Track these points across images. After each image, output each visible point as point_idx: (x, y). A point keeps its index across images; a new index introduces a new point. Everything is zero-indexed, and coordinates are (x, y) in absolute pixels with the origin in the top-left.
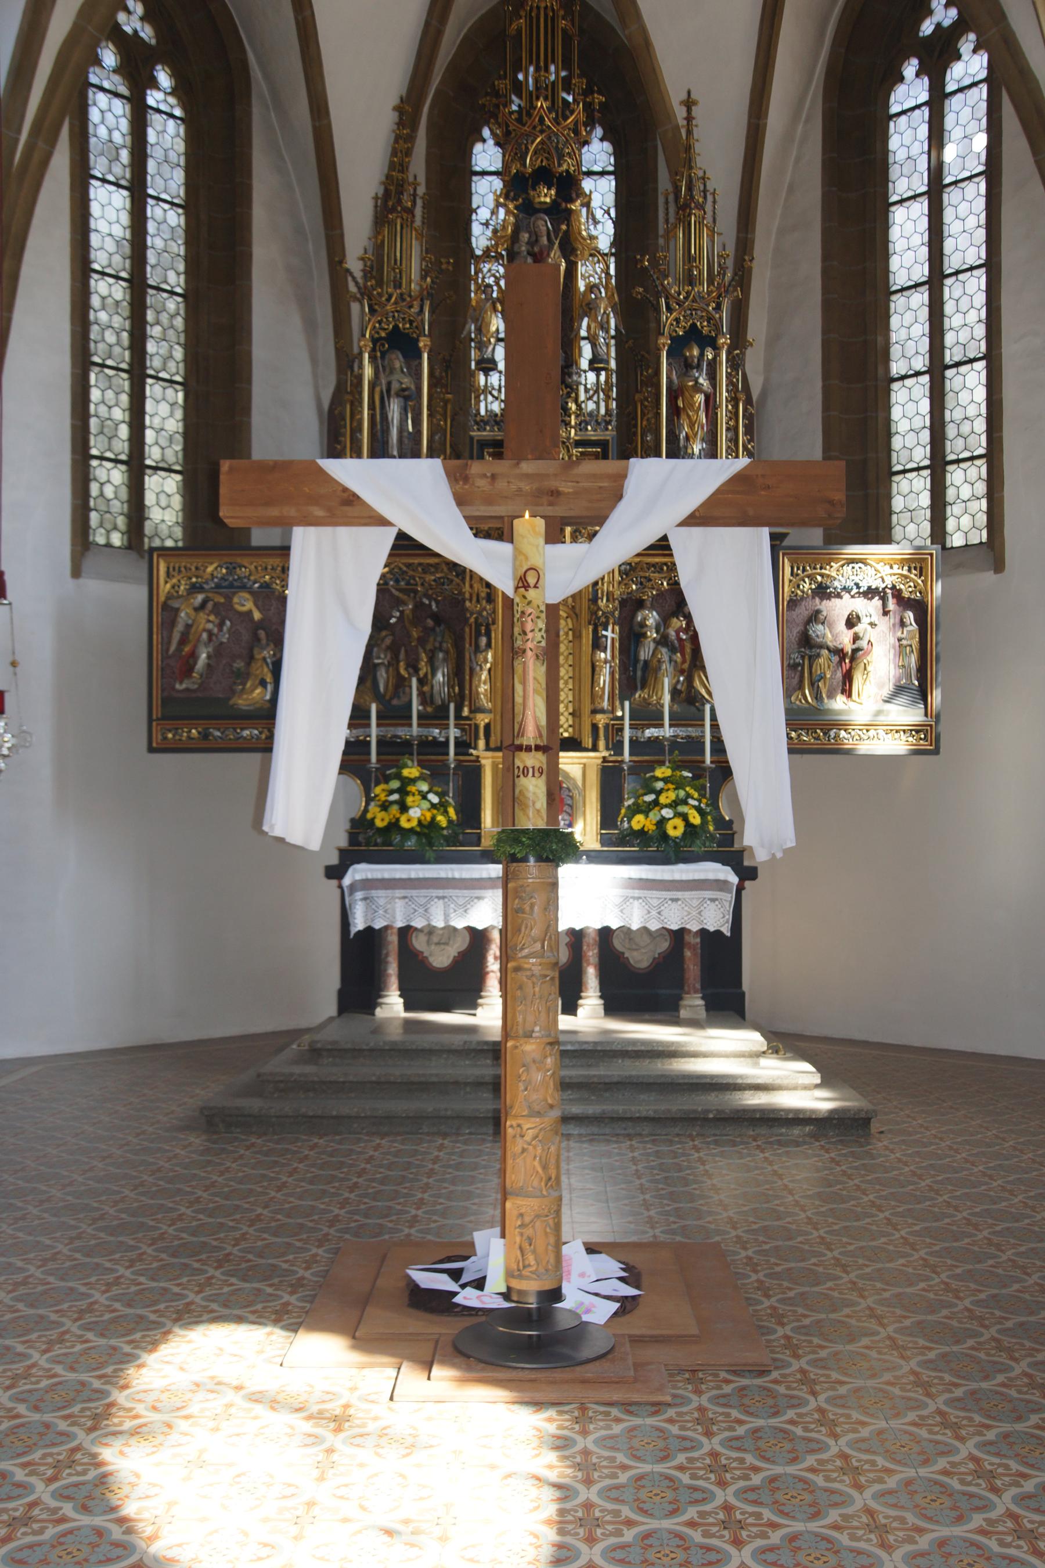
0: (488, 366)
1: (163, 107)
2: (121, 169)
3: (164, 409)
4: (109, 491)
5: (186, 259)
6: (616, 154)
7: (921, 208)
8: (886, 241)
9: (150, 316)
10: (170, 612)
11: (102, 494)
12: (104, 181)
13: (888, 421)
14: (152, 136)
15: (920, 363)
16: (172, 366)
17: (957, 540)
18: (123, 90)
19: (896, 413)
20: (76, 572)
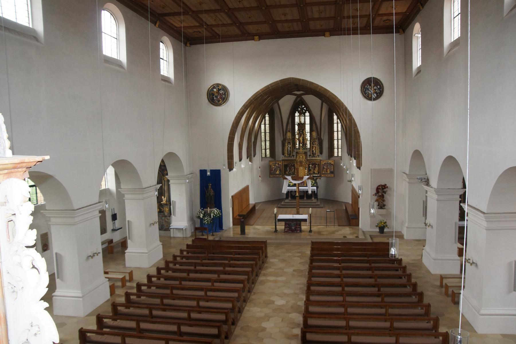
0: (297, 144)
3: (268, 143)
4: (263, 152)
5: (269, 129)
6: (309, 114)
7: (336, 124)
8: (334, 127)
10: (271, 166)
13: (334, 143)
15: (337, 139)
17: (339, 155)
19: (335, 143)
20: (262, 161)
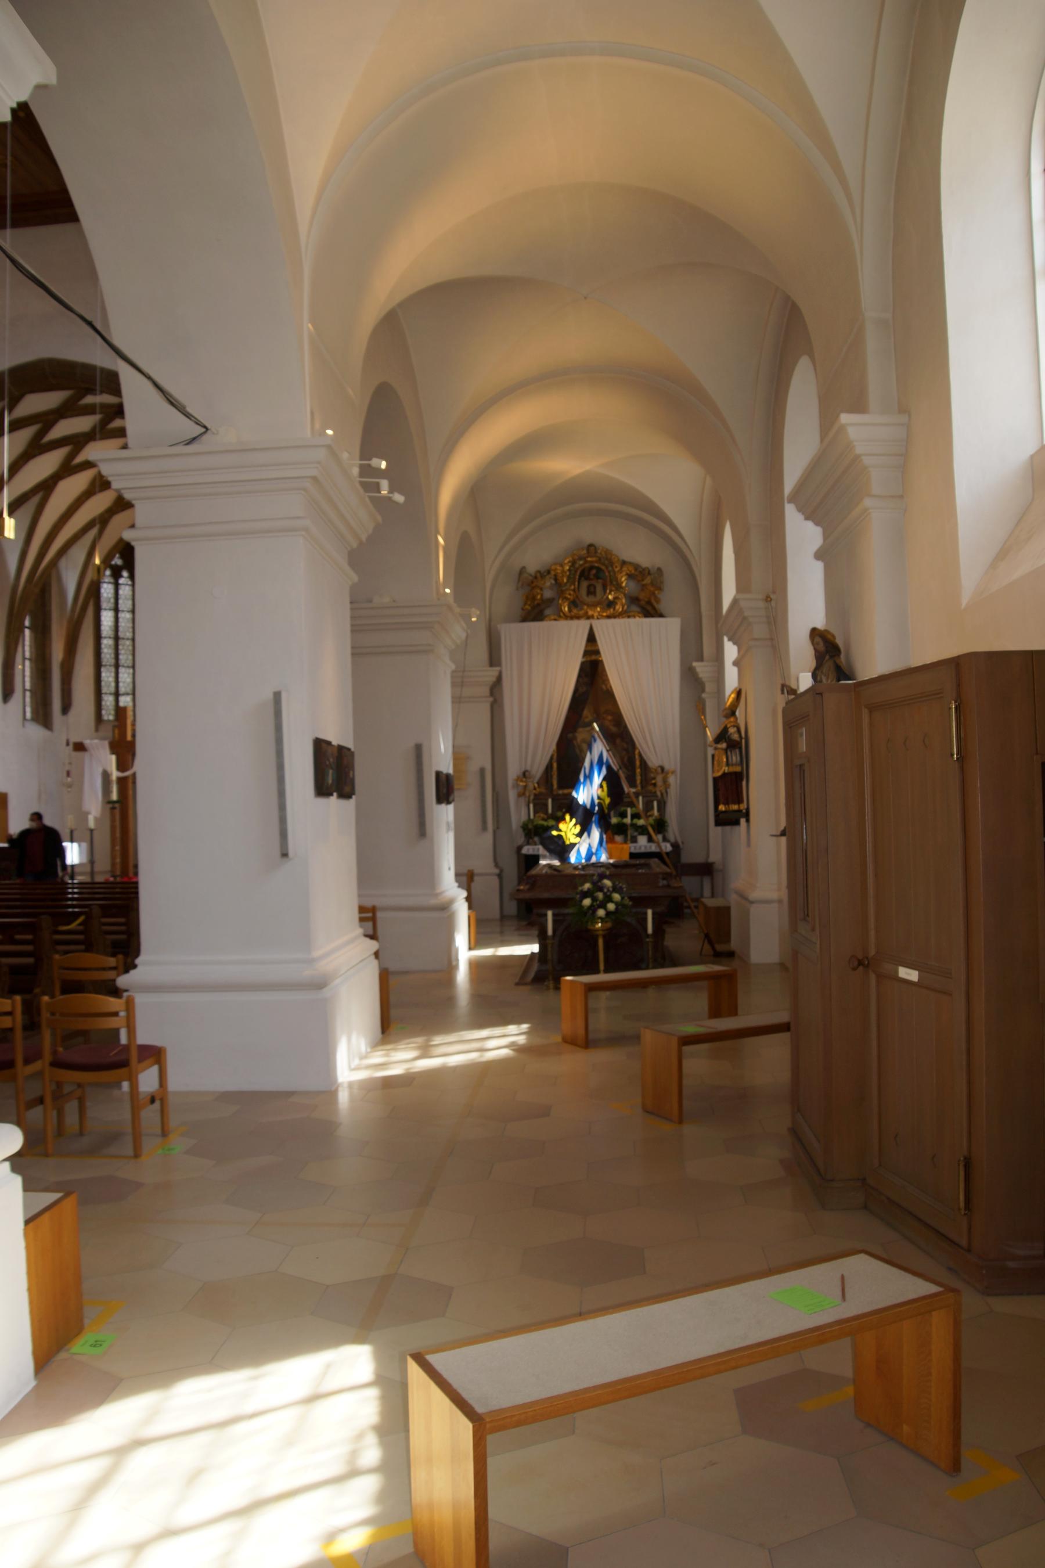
1: (125, 583)
2: (111, 605)
3: (126, 675)
4: (108, 703)
9: (120, 647)
11: (106, 705)
12: (105, 609)
14: (121, 592)
16: (128, 662)
18: (112, 580)
